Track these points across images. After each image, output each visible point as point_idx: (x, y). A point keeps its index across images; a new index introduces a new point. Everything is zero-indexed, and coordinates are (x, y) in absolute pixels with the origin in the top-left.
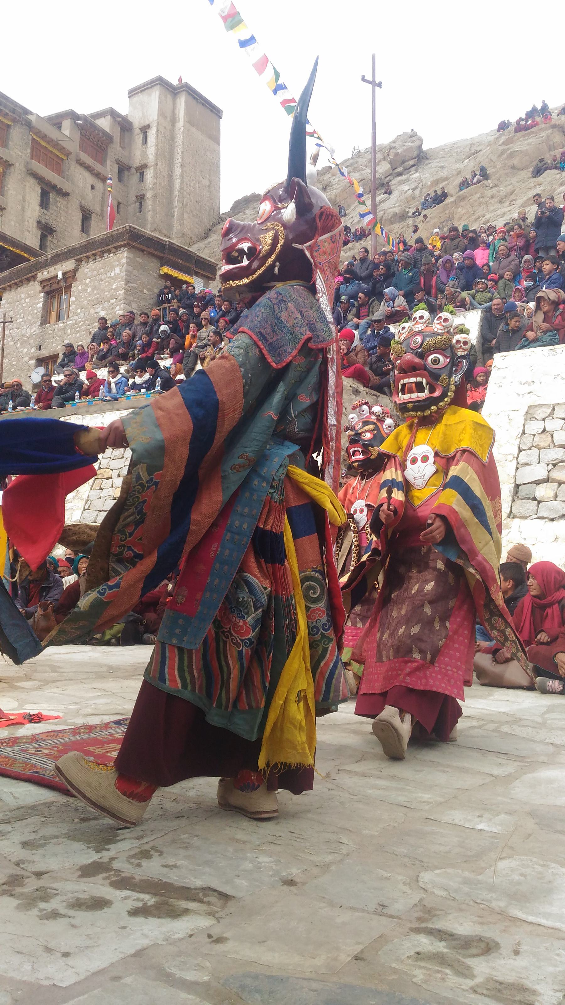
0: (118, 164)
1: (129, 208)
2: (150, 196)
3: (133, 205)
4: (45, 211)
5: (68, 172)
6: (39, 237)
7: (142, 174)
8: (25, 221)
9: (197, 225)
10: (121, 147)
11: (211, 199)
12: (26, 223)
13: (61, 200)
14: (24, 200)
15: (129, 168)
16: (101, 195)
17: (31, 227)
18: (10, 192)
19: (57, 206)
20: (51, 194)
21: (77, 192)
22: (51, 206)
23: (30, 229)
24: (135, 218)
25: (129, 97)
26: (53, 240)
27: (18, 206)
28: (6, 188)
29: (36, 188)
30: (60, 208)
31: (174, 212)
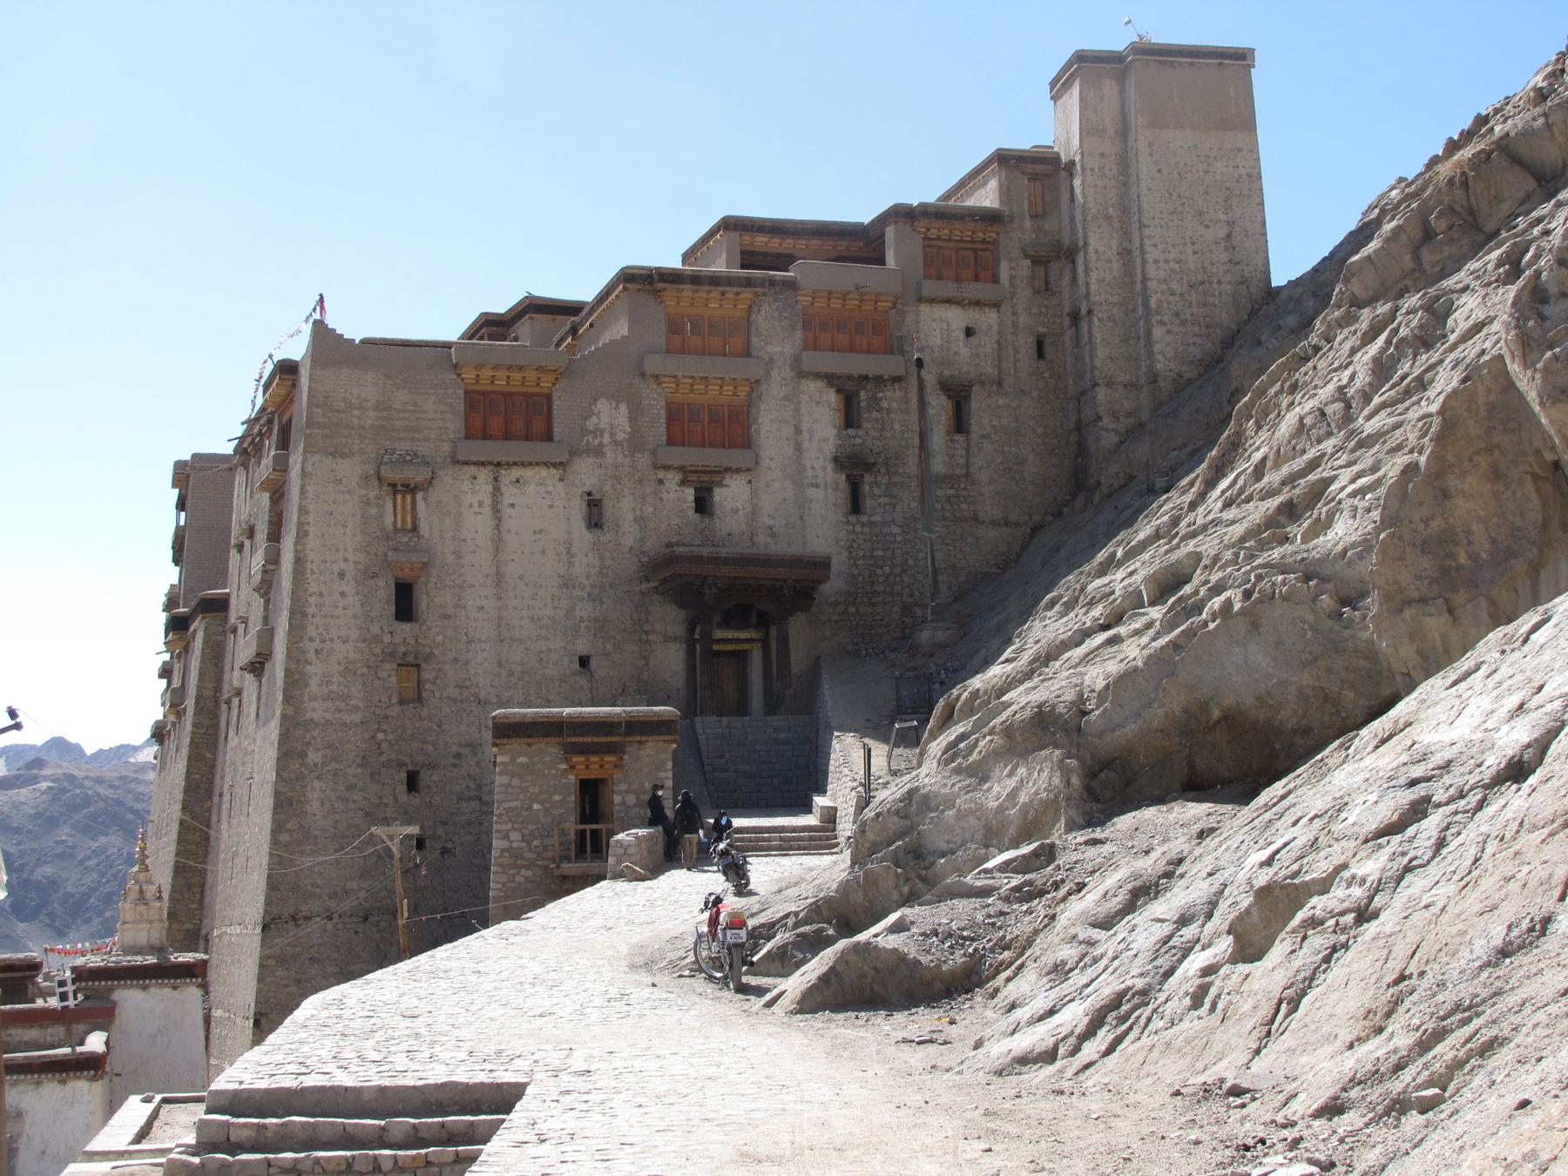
0: (1027, 257)
4: (851, 432)
7: (1073, 262)
9: (1197, 340)
11: (1237, 263)
14: (798, 431)
17: (820, 473)
18: (763, 433)
19: (880, 410)
20: (862, 393)
22: (865, 416)
23: (819, 481)
25: (1055, 98)
28: (754, 427)
30: (889, 410)
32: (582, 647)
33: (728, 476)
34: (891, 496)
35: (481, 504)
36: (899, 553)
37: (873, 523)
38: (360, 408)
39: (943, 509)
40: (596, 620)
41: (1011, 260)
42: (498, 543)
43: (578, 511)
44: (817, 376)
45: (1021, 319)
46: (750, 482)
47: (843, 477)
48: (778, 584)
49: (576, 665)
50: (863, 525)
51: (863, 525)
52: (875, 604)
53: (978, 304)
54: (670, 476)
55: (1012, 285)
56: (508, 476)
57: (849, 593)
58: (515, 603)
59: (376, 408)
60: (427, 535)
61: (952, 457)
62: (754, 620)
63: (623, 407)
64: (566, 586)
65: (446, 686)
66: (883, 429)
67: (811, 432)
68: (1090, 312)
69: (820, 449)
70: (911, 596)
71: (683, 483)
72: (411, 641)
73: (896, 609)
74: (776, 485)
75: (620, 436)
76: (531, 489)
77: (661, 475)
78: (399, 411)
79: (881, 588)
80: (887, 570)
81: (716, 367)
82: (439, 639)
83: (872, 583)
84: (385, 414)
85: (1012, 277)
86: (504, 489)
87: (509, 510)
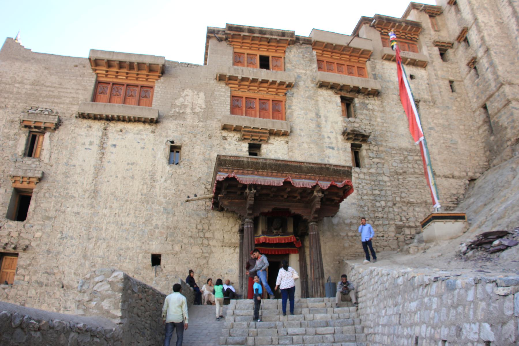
0: (437, 46)
1: (466, 81)
2: (483, 54)
3: (469, 75)
4: (350, 119)
7: (466, 40)
8: (324, 138)
12: (327, 140)
13: (373, 102)
14: (318, 115)
15: (451, 45)
16: (427, 82)
17: (335, 141)
18: (295, 114)
19: (368, 110)
20: (356, 100)
21: (392, 87)
22: (359, 112)
23: (333, 145)
24: (475, 87)
26: (372, 147)
27: (311, 125)
28: (289, 111)
29: (333, 99)
30: (373, 110)
33: (272, 138)
35: (91, 143)
37: (371, 173)
38: (21, 83)
39: (414, 168)
40: (168, 227)
41: (428, 47)
42: (98, 170)
45: (439, 73)
46: (287, 142)
47: (348, 145)
49: (149, 261)
50: (364, 174)
51: (364, 174)
52: (377, 226)
53: (414, 63)
54: (231, 134)
55: (431, 57)
56: (114, 127)
58: (105, 211)
59: (33, 84)
60: (46, 161)
62: (291, 229)
63: (202, 95)
65: (36, 272)
66: (370, 120)
67: (326, 117)
68: (487, 50)
72: (15, 234)
73: (392, 228)
74: (305, 145)
75: (198, 110)
76: (130, 136)
77: (225, 133)
78: (48, 86)
79: (380, 215)
82: (38, 234)
84: (38, 88)
85: (430, 54)
86: (110, 135)
87: (112, 149)
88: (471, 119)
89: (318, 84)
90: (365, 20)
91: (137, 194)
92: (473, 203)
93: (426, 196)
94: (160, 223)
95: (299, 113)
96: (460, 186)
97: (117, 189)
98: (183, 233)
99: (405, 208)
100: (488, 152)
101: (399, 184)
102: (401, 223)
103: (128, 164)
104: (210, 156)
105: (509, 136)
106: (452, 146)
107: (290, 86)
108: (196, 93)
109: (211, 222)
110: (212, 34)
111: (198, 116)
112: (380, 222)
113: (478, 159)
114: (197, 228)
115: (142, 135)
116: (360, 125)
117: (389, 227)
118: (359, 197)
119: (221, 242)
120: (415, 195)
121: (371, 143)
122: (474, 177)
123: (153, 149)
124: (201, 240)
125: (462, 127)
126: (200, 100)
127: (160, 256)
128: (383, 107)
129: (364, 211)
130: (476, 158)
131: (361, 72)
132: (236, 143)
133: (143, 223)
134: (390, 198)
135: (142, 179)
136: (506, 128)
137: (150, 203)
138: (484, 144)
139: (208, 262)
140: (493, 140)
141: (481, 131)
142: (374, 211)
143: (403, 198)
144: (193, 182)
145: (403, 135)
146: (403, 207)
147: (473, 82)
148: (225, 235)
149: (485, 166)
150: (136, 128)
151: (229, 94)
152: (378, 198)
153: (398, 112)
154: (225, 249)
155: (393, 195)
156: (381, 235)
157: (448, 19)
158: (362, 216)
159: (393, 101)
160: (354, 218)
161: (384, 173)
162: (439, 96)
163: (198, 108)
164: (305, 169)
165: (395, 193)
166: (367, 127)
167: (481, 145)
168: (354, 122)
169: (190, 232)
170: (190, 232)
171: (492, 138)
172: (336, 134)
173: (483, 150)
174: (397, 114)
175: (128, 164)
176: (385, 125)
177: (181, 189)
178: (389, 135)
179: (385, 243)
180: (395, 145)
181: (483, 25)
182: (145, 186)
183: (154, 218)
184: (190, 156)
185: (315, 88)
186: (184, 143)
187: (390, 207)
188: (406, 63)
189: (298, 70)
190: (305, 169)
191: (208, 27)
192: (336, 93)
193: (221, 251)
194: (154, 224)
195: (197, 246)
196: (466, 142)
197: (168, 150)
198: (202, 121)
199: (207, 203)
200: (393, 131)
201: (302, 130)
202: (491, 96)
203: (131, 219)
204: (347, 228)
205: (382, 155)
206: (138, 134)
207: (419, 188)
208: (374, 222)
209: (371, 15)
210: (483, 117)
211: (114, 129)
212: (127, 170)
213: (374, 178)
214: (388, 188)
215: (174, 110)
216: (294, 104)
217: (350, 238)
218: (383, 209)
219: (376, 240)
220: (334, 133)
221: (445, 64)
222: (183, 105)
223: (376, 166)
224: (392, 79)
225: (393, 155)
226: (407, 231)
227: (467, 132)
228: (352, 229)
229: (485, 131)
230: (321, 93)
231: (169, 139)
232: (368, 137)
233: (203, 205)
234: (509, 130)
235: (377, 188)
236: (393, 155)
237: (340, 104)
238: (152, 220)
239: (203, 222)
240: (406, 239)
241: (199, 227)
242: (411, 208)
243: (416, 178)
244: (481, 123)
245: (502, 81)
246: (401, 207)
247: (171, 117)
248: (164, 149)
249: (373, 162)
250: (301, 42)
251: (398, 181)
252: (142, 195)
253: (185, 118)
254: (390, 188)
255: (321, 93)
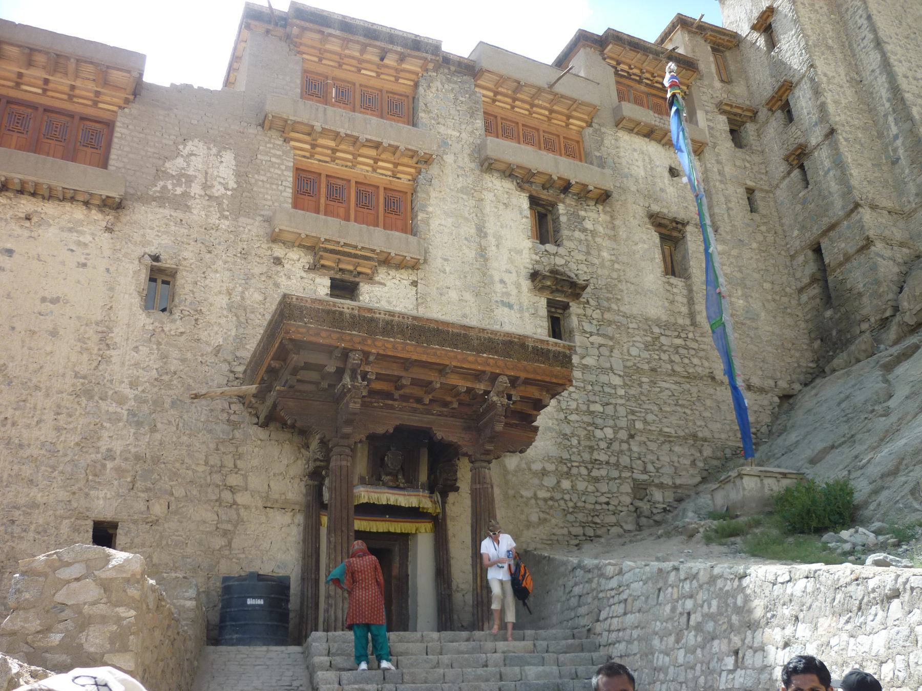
0: (723, 112)
4: (549, 247)
5: (599, 150)
6: (543, 311)
8: (492, 283)
10: (722, 81)
13: (593, 215)
14: (481, 231)
17: (514, 292)
18: (434, 224)
19: (584, 230)
20: (561, 208)
22: (565, 232)
23: (513, 300)
24: (799, 207)
26: (589, 312)
27: (466, 251)
28: (421, 216)
30: (594, 233)
31: (895, 150)
32: (104, 506)
33: (382, 271)
34: (604, 336)
36: (622, 411)
40: (138, 458)
41: (707, 112)
43: (131, 280)
44: (509, 172)
45: (728, 169)
47: (543, 302)
48: (481, 387)
52: (597, 480)
55: (712, 136)
57: (561, 461)
61: (672, 302)
63: (228, 157)
64: (89, 394)
66: (588, 253)
67: (499, 238)
69: (511, 261)
70: (645, 471)
71: (314, 268)
73: (627, 488)
74: (453, 295)
75: (218, 191)
76: (51, 233)
77: (279, 251)
79: (603, 457)
80: (609, 432)
81: (371, 127)
83: (591, 449)
88: (786, 271)
89: (486, 165)
90: (583, 39)
91: (64, 375)
92: (797, 443)
93: (695, 424)
94: (118, 446)
95: (443, 222)
96: (761, 406)
97: (12, 358)
98: (175, 474)
99: (653, 446)
100: (819, 342)
101: (641, 393)
102: (645, 477)
103: (44, 300)
104: (243, 298)
105: (865, 312)
106: (748, 322)
107: (427, 160)
108: (214, 151)
109: (240, 449)
110: (255, 18)
111: (220, 205)
112: (603, 472)
113: (797, 354)
114: (206, 464)
115: (82, 233)
116: (567, 263)
117: (621, 484)
118: (562, 416)
119: (261, 497)
120: (674, 419)
121: (588, 302)
122: (791, 392)
123: (108, 270)
124: (217, 491)
125: (767, 286)
126: (225, 169)
127: (114, 525)
128: (614, 228)
129: (571, 446)
130: (793, 352)
131: (574, 149)
132: (304, 275)
133: (77, 444)
134: (623, 423)
135: (79, 340)
136: (860, 295)
137: (96, 398)
138: (810, 325)
139: (230, 543)
140: (831, 319)
141: (804, 298)
142: (591, 447)
143: (649, 424)
144: (202, 355)
145: (651, 292)
146: (648, 443)
147: (795, 196)
148: (272, 484)
149: (811, 371)
150: (67, 217)
151: (292, 164)
152: (599, 421)
153: (644, 242)
154: (270, 515)
155: (630, 417)
156: (603, 499)
157: (749, 61)
158: (566, 456)
159: (634, 217)
160: (549, 459)
161: (611, 369)
162: (726, 217)
163: (218, 187)
164: (475, 342)
165: (633, 413)
166: (580, 267)
167: (803, 325)
168: (554, 255)
169: (190, 472)
170: (190, 472)
171: (828, 313)
172: (518, 276)
173: (806, 336)
174: (640, 245)
175: (44, 300)
176: (616, 266)
177: (173, 369)
178: (623, 286)
179: (612, 519)
180: (635, 311)
181: (825, 79)
182: (85, 357)
183: (105, 434)
184: (196, 295)
185: (477, 172)
186: (184, 263)
187: (622, 441)
188: (663, 142)
189: (442, 129)
190: (475, 342)
191: (247, 4)
192: (521, 187)
193: (263, 519)
194: (103, 449)
195: (206, 506)
196: (775, 317)
197: (144, 276)
198: (227, 218)
199: (233, 406)
200: (634, 280)
201: (446, 260)
202: (832, 227)
203: (46, 433)
204: (536, 481)
205: (610, 330)
206: (70, 230)
207: (682, 406)
208: (590, 471)
209: (600, 31)
210: (811, 268)
211: (11, 213)
212: (40, 314)
213: (593, 378)
214: (620, 401)
215: (162, 183)
216: (432, 201)
217: (541, 503)
218: (610, 445)
219: (593, 510)
220: (514, 274)
221: (739, 153)
222: (183, 175)
223: (596, 352)
224: (633, 172)
225: (630, 330)
226: (658, 496)
227: (777, 298)
228: (545, 484)
229: (814, 298)
230: (490, 185)
231: (147, 250)
232: (584, 288)
233: (223, 410)
234: (865, 300)
235: (597, 399)
236: (630, 330)
237: (527, 212)
238: (99, 439)
239: (222, 449)
240: (655, 511)
241: (214, 460)
242: (666, 447)
243: (676, 383)
244: (806, 280)
245: (858, 199)
246: (645, 443)
247: (154, 199)
248: (135, 272)
249: (592, 343)
250: (453, 68)
251: (641, 387)
252: (76, 377)
253: (186, 205)
254: (623, 401)
255: (490, 185)
